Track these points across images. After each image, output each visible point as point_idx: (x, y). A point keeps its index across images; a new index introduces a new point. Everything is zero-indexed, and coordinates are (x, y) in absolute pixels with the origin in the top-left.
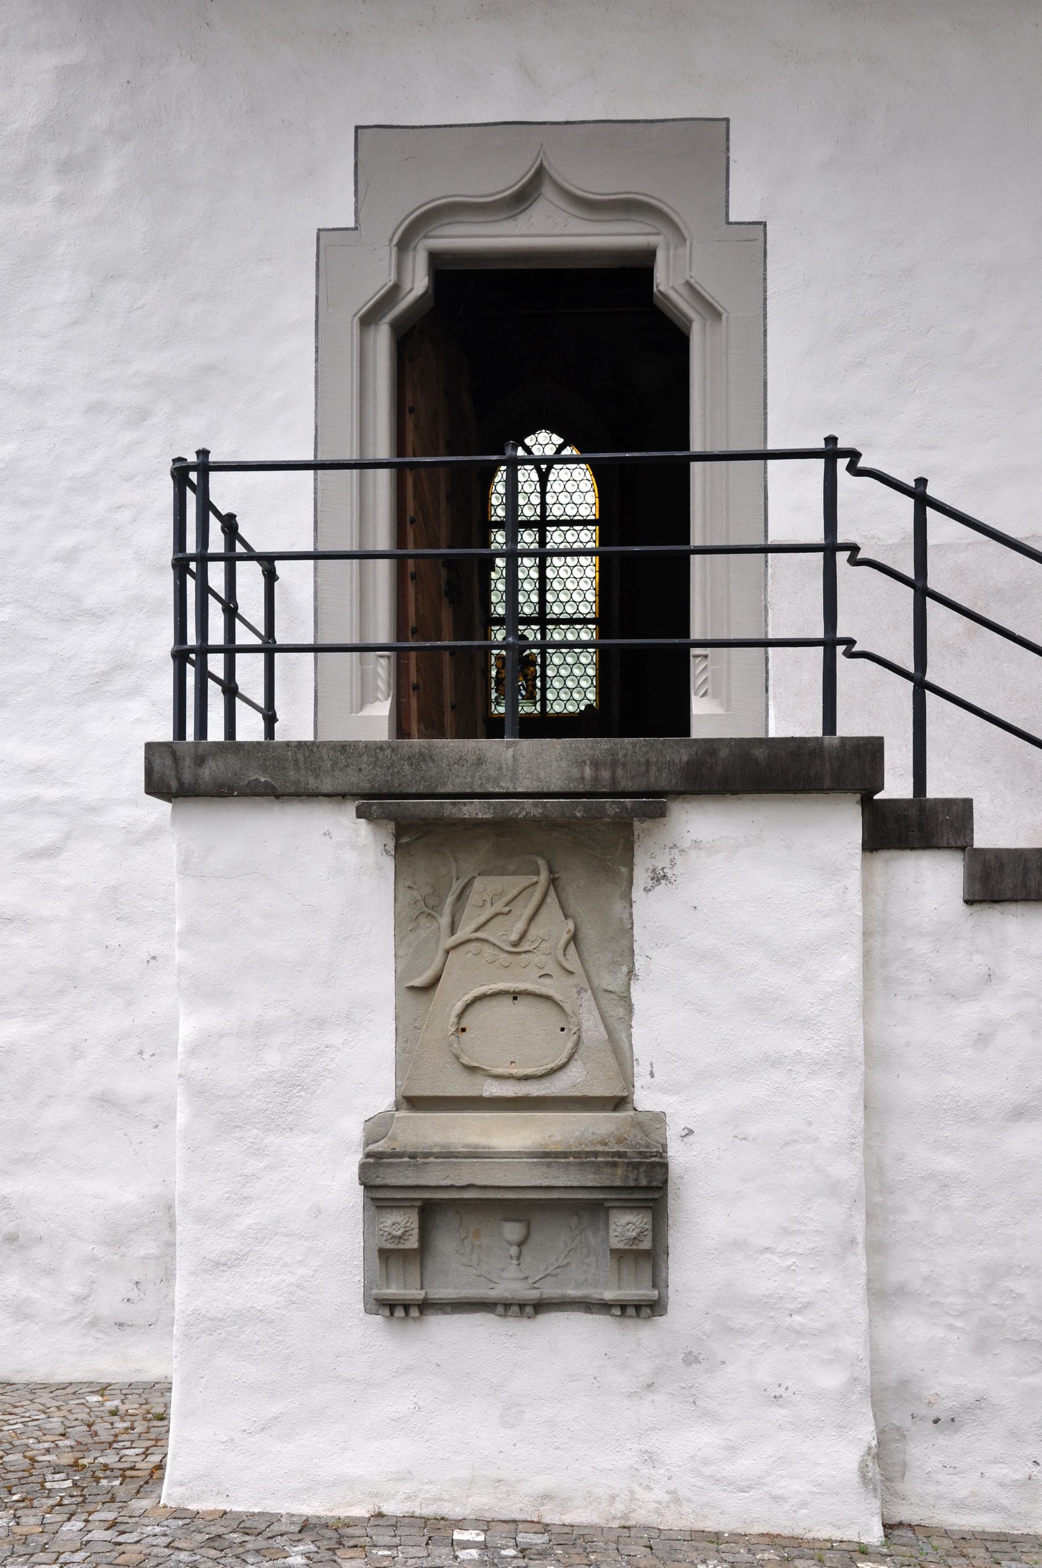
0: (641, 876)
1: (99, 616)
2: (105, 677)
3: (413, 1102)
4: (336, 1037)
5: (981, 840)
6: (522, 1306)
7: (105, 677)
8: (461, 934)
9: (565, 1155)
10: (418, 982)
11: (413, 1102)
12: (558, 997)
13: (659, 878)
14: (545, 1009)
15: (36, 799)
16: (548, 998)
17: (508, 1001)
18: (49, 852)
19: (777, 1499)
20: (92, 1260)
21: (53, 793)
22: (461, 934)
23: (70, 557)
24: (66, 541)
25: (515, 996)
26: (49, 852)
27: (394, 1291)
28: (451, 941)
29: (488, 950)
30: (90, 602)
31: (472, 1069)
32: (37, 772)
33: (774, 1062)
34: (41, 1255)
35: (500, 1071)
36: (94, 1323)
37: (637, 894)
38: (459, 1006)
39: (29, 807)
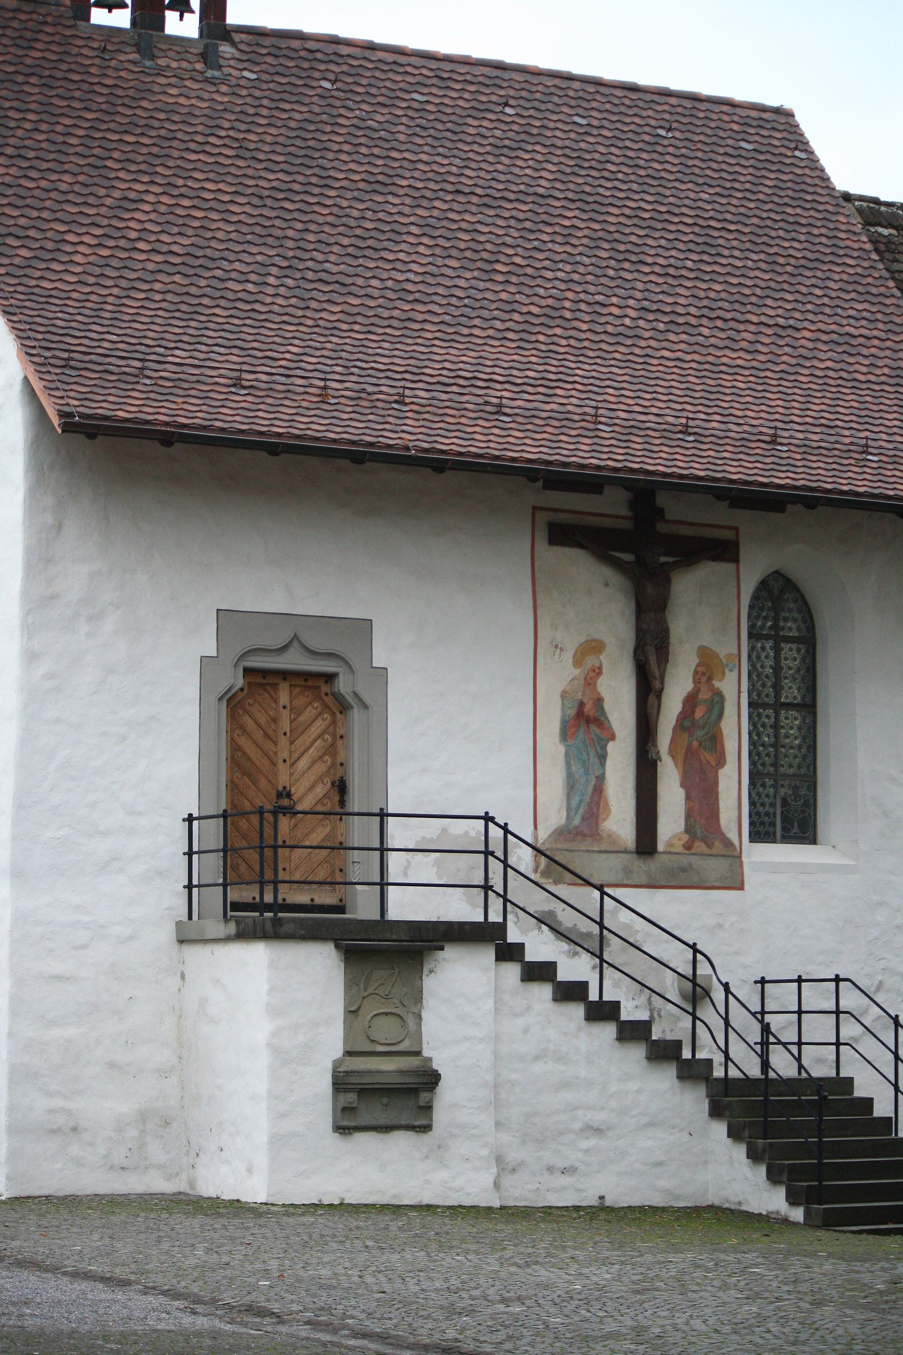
0: (425, 971)
3: (349, 1053)
5: (528, 958)
6: (387, 1128)
8: (370, 991)
9: (408, 1072)
10: (352, 1009)
12: (402, 1015)
13: (431, 971)
14: (399, 1020)
16: (399, 1015)
17: (384, 1016)
18: (83, 947)
19: (468, 1194)
22: (370, 991)
25: (387, 1014)
26: (83, 947)
27: (345, 1123)
28: (366, 994)
29: (378, 997)
31: (373, 1041)
33: (467, 1039)
35: (382, 1042)
36: (111, 1168)
37: (424, 977)
38: (369, 1018)
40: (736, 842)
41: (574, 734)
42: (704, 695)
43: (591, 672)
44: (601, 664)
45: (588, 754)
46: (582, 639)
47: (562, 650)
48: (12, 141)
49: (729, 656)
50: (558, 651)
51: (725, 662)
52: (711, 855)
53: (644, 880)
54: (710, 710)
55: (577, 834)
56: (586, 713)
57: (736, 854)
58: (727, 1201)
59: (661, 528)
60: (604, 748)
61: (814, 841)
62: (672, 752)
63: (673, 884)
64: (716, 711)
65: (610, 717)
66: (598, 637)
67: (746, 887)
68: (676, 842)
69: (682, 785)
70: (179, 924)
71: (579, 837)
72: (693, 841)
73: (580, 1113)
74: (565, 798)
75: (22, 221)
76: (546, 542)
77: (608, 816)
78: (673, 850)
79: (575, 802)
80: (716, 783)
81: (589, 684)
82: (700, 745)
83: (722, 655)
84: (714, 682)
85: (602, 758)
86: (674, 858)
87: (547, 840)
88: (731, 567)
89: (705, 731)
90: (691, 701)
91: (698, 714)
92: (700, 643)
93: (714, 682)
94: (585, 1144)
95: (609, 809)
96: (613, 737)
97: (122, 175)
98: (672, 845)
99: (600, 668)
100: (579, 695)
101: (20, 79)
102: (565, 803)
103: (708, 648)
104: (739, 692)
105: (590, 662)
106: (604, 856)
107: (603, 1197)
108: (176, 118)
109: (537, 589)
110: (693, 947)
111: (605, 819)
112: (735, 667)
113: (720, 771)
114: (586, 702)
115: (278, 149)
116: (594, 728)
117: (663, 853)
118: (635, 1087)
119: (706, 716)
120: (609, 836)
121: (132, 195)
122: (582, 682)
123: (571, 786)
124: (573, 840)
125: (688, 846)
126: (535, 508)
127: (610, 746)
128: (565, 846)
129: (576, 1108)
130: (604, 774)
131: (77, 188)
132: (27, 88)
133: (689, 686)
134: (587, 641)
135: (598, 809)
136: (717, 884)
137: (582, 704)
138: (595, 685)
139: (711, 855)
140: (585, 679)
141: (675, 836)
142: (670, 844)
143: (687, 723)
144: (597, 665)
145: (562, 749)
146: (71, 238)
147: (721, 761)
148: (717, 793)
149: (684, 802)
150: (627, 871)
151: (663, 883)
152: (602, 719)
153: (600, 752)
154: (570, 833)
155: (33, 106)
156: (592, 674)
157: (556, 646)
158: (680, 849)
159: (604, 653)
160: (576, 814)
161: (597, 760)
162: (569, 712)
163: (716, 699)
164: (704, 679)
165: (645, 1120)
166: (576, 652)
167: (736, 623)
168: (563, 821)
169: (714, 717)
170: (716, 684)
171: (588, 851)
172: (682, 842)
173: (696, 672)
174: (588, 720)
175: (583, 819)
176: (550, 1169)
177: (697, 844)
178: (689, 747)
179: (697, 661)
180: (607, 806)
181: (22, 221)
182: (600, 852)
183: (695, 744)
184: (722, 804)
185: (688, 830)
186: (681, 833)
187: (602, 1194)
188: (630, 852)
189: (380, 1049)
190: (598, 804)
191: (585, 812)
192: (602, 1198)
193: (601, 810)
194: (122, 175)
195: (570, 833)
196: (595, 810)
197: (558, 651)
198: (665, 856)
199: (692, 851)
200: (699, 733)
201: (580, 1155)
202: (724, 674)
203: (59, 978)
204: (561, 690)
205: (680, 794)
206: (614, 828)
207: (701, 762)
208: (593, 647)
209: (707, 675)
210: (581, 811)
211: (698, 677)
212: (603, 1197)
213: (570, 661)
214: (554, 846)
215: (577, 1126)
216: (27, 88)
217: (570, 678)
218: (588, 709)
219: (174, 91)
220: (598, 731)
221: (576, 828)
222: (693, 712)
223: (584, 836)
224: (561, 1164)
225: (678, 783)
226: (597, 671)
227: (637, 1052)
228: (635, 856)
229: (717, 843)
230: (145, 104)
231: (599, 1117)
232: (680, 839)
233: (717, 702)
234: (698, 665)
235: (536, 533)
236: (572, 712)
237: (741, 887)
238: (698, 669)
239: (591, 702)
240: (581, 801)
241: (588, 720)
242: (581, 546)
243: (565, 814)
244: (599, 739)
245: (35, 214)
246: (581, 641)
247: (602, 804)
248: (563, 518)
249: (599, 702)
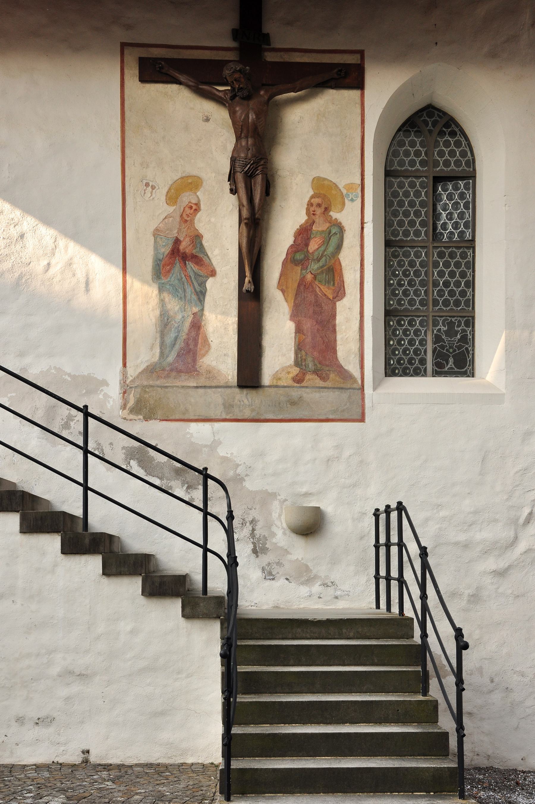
40: (356, 374)
41: (169, 271)
42: (320, 226)
43: (187, 209)
44: (199, 201)
45: (185, 291)
46: (176, 176)
47: (153, 188)
49: (350, 187)
50: (149, 189)
51: (344, 192)
52: (325, 388)
53: (247, 414)
54: (326, 242)
55: (172, 370)
56: (182, 251)
57: (355, 386)
59: (270, 57)
60: (203, 284)
62: (282, 286)
63: (280, 417)
64: (334, 241)
65: (209, 254)
66: (194, 173)
67: (367, 419)
68: (283, 375)
69: (294, 316)
71: (174, 374)
72: (304, 374)
74: (158, 335)
76: (137, 79)
77: (207, 352)
78: (280, 383)
79: (169, 340)
80: (334, 316)
81: (186, 221)
82: (315, 277)
83: (341, 186)
84: (331, 213)
85: (201, 295)
86: (281, 391)
87: (138, 377)
88: (355, 94)
89: (321, 263)
91: (313, 246)
92: (315, 174)
93: (331, 213)
95: (209, 345)
96: (213, 273)
98: (280, 379)
99: (198, 204)
100: (175, 233)
102: (158, 340)
103: (325, 179)
104: (362, 223)
105: (187, 198)
106: (201, 391)
107: (88, 752)
109: (127, 128)
110: (205, 475)
111: (204, 355)
112: (357, 197)
113: (339, 305)
114: (182, 239)
116: (190, 265)
117: (270, 386)
119: (322, 248)
120: (209, 372)
122: (178, 219)
124: (168, 376)
125: (298, 380)
126: (124, 46)
127: (210, 283)
128: (158, 383)
133: (302, 218)
134: (182, 178)
135: (196, 345)
136: (331, 417)
137: (177, 242)
138: (192, 222)
139: (325, 388)
140: (181, 216)
141: (283, 369)
142: (276, 377)
143: (299, 256)
144: (194, 201)
148: (334, 326)
149: (293, 335)
150: (228, 406)
151: (271, 417)
152: (201, 255)
153: (198, 288)
154: (164, 370)
156: (188, 211)
157: (147, 185)
158: (290, 383)
159: (202, 189)
160: (170, 351)
161: (194, 297)
162: (163, 250)
163: (333, 231)
164: (319, 211)
166: (170, 189)
167: (359, 152)
168: (156, 358)
169: (331, 249)
170: (334, 215)
171: (183, 387)
172: (291, 375)
173: (310, 204)
174: (185, 258)
175: (178, 356)
176: (20, 720)
177: (308, 377)
178: (303, 279)
179: (311, 193)
180: (206, 341)
182: (197, 387)
183: (309, 277)
185: (297, 363)
186: (290, 366)
187: (86, 748)
188: (235, 387)
190: (196, 341)
191: (181, 349)
193: (199, 346)
195: (164, 370)
196: (191, 347)
197: (149, 189)
198: (270, 390)
199: (302, 385)
200: (314, 266)
202: (344, 204)
204: (152, 229)
205: (290, 326)
206: (214, 364)
207: (316, 295)
209: (323, 206)
210: (177, 347)
211: (312, 209)
212: (88, 752)
213: (163, 198)
214: (145, 383)
217: (163, 216)
218: (185, 246)
220: (196, 268)
221: (170, 364)
222: (307, 245)
223: (179, 372)
224: (33, 713)
225: (288, 316)
226: (194, 207)
228: (237, 390)
229: (332, 376)
232: (289, 373)
233: (335, 234)
234: (312, 197)
235: (126, 71)
236: (166, 250)
237: (362, 419)
238: (312, 201)
239: (188, 239)
240: (176, 338)
241: (185, 258)
243: (158, 351)
244: (197, 275)
246: (176, 178)
247: (200, 341)
248: (156, 53)
249: (197, 238)
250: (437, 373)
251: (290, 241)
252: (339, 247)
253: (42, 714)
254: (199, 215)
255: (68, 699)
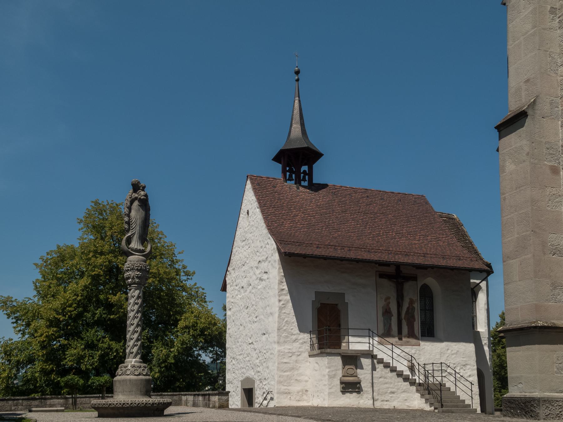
1: (294, 335)
2: (295, 340)
4: (338, 371)
7: (295, 340)
11: (343, 376)
15: (289, 352)
16: (353, 369)
18: (291, 357)
20: (296, 395)
21: (291, 351)
23: (292, 329)
24: (292, 328)
26: (291, 357)
30: (294, 333)
32: (289, 349)
33: (366, 373)
34: (292, 394)
39: (289, 352)
48: (273, 205)
58: (420, 408)
61: (434, 337)
62: (405, 319)
70: (309, 352)
73: (389, 389)
75: (275, 219)
85: (391, 320)
90: (408, 308)
94: (391, 395)
96: (393, 316)
97: (294, 210)
101: (274, 193)
108: (304, 200)
115: (324, 205)
118: (401, 384)
121: (296, 214)
123: (384, 326)
127: (392, 318)
129: (388, 388)
130: (391, 323)
131: (286, 213)
132: (275, 195)
137: (386, 309)
145: (383, 319)
146: (285, 222)
147: (415, 321)
155: (277, 198)
165: (403, 391)
180: (392, 330)
181: (275, 219)
184: (415, 329)
189: (349, 375)
192: (394, 407)
194: (294, 210)
201: (390, 398)
203: (286, 363)
205: (407, 326)
208: (388, 298)
215: (389, 392)
216: (275, 195)
219: (304, 195)
224: (386, 399)
227: (401, 379)
230: (298, 198)
231: (393, 390)
242: (385, 278)
245: (278, 218)
249: (390, 309)
250: (428, 336)
251: (406, 310)
252: (414, 311)
253: (387, 400)
254: (390, 304)
255: (391, 397)
